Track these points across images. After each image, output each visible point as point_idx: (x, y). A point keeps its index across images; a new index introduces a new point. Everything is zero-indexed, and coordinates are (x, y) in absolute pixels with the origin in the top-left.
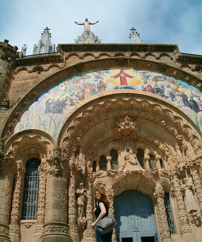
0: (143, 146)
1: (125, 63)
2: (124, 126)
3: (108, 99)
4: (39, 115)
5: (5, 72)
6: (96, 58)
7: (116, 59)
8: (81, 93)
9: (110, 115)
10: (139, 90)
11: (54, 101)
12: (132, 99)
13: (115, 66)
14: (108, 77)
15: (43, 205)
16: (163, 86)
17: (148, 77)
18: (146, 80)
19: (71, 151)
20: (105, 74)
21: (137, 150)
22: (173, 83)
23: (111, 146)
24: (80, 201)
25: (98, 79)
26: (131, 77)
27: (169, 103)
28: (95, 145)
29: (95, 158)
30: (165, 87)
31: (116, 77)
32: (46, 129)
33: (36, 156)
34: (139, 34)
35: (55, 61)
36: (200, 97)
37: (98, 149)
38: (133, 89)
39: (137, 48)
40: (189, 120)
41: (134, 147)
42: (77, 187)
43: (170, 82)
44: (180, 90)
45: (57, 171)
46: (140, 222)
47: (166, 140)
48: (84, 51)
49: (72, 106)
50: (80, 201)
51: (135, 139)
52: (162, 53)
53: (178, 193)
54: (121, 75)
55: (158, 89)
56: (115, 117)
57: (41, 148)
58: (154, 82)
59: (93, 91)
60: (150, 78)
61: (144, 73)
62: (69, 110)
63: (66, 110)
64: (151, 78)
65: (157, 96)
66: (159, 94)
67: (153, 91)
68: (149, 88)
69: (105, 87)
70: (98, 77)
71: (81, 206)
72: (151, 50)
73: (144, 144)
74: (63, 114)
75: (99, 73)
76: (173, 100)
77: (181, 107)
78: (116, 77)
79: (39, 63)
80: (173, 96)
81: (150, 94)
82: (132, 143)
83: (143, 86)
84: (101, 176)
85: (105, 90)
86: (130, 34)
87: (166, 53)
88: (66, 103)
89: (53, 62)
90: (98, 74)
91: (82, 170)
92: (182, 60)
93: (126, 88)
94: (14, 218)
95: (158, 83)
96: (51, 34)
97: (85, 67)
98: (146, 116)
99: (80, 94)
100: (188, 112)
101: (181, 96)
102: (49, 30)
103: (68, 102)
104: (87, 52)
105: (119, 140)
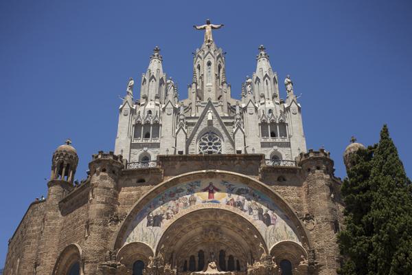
5: (113, 186)
9: (198, 225)
13: (206, 178)
17: (233, 189)
20: (197, 187)
23: (200, 248)
26: (218, 190)
48: (180, 161)
62: (166, 224)
65: (237, 211)
67: (234, 205)
69: (195, 201)
72: (240, 159)
78: (205, 190)
80: (251, 210)
81: (231, 208)
103: (165, 216)
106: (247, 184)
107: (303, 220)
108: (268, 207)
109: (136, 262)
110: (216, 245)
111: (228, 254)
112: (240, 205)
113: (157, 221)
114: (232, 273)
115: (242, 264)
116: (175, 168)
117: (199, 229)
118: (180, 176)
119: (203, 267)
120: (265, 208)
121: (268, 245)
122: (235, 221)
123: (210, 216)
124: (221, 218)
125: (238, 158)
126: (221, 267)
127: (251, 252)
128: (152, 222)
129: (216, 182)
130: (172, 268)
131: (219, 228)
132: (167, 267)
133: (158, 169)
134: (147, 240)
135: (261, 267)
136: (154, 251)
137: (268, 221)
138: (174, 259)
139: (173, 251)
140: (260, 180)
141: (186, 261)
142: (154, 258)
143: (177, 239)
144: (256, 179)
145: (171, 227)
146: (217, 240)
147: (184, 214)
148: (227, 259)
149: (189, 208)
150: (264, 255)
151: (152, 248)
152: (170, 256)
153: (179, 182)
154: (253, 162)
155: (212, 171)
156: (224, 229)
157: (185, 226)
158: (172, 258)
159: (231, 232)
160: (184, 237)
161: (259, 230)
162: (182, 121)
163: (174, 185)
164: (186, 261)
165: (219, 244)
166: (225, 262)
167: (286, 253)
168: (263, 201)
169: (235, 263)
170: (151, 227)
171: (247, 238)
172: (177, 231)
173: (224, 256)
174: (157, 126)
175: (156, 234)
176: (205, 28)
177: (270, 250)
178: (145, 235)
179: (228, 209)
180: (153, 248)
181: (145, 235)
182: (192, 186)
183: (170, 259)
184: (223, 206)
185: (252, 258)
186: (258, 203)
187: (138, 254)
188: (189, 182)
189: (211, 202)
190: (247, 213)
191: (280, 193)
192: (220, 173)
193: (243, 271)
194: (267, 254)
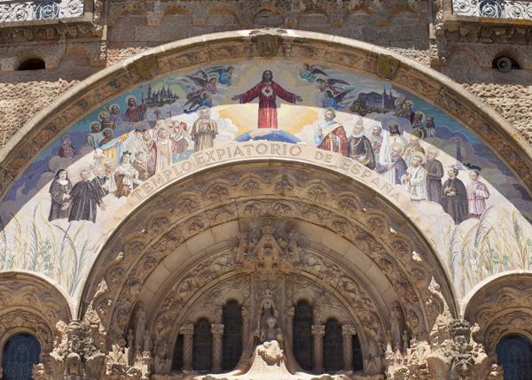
0: (313, 295)
1: (280, 50)
4: (34, 226)
8: (145, 155)
9: (223, 217)
11: (74, 181)
13: (250, 57)
14: (224, 97)
17: (340, 98)
19: (115, 323)
20: (219, 86)
21: (293, 309)
22: (412, 118)
23: (228, 293)
25: (198, 105)
26: (291, 98)
28: (183, 294)
29: (182, 328)
32: (50, 267)
33: (33, 333)
35: (77, 37)
38: (288, 141)
41: (286, 296)
47: (374, 285)
49: (119, 197)
51: (293, 274)
54: (263, 91)
55: (362, 142)
56: (238, 219)
57: (40, 315)
59: (180, 146)
61: (332, 81)
62: (113, 211)
63: (103, 209)
65: (355, 169)
66: (362, 158)
67: (346, 149)
68: (338, 139)
69: (213, 134)
70: (199, 97)
73: (316, 289)
74: (94, 222)
76: (398, 182)
77: (416, 203)
78: (246, 98)
79: (32, 40)
80: (401, 166)
81: (334, 161)
83: (321, 130)
85: (212, 146)
88: (103, 186)
89: (73, 40)
97: (161, 65)
99: (145, 158)
101: (423, 165)
103: (110, 185)
105: (249, 275)
106: (390, 78)
108: (459, 157)
109: (14, 337)
110: (282, 284)
111: (322, 314)
112: (363, 148)
113: (82, 201)
114: (335, 377)
115: (369, 349)
116: (146, 21)
117: (227, 230)
118: (163, 48)
119: (235, 358)
120: (448, 161)
121: (456, 285)
122: (346, 203)
123: (263, 186)
124: (301, 193)
126: (299, 357)
127: (400, 308)
128: (66, 206)
129: (286, 73)
130: (132, 361)
131: (291, 226)
132: (117, 356)
133: (88, 25)
134: (50, 267)
135: (431, 360)
136: (74, 302)
137: (457, 204)
138: (140, 328)
139: (137, 307)
140: (435, 65)
141: (181, 337)
142: (73, 326)
143: (151, 262)
144: (419, 61)
145: (129, 224)
146: (287, 266)
147: (175, 178)
148: (318, 331)
150: (444, 319)
151: (63, 289)
152: (125, 320)
153: (159, 71)
155: (273, 32)
156: (310, 229)
157: (178, 218)
158: (132, 326)
159: (333, 242)
160: (175, 258)
161: (429, 237)
163: (142, 78)
164: (181, 337)
165: (293, 279)
166: (312, 337)
167: (518, 314)
168: (443, 137)
170: (64, 222)
171: (387, 262)
172: (152, 238)
173: (311, 321)
175: (78, 244)
177: (463, 302)
178: (43, 250)
179: (319, 163)
180: (71, 291)
181: (43, 250)
182: (201, 82)
183: (128, 331)
184: (307, 153)
185: (403, 327)
186: (425, 144)
187: (18, 313)
188: (193, 70)
189: (268, 137)
191: (499, 110)
192: (297, 41)
193: (372, 374)
194: (454, 313)
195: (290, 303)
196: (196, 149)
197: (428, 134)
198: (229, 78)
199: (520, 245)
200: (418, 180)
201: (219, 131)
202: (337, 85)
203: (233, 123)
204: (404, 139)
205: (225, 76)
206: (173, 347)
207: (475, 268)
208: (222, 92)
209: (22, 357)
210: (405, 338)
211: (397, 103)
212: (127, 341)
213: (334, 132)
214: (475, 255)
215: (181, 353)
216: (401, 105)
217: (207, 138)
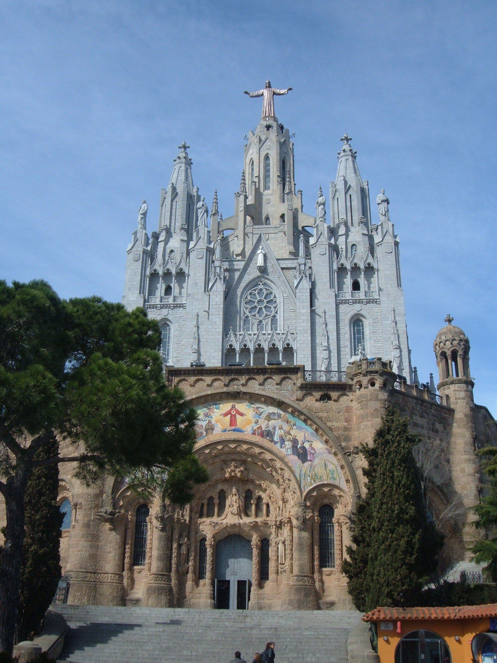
2: (230, 473)
3: (213, 446)
6: (208, 386)
7: (228, 393)
9: (217, 460)
10: (247, 435)
12: (239, 445)
13: (227, 399)
14: (217, 415)
15: (150, 555)
16: (274, 428)
17: (260, 414)
18: (258, 419)
20: (215, 410)
21: (245, 494)
22: (288, 422)
23: (220, 487)
24: (184, 550)
26: (242, 415)
27: (276, 452)
28: (203, 488)
30: (277, 429)
31: (226, 415)
34: (356, 153)
36: (312, 442)
37: (207, 490)
39: (255, 371)
40: (293, 472)
42: (180, 536)
43: (284, 421)
44: (293, 432)
45: (161, 528)
46: (239, 567)
50: (184, 550)
51: (244, 480)
52: (284, 376)
53: (273, 544)
54: (232, 412)
56: (223, 460)
58: (266, 421)
60: (262, 416)
61: (258, 408)
64: (264, 416)
65: (265, 442)
66: (268, 438)
67: (262, 435)
68: (259, 431)
69: (213, 429)
71: (184, 554)
72: (271, 373)
75: (209, 409)
76: (281, 447)
77: (288, 456)
78: (226, 415)
80: (282, 441)
81: (257, 439)
82: (241, 484)
83: (253, 427)
84: (204, 524)
86: (339, 154)
87: (289, 376)
90: (208, 411)
91: (185, 521)
92: (306, 387)
93: (234, 430)
94: (126, 566)
95: (272, 423)
96: (190, 160)
97: (194, 403)
98: (253, 460)
100: (294, 462)
101: (291, 441)
102: (189, 147)
104: (198, 377)
107: (349, 455)
125: (269, 371)
149: (206, 438)
154: (289, 376)
162: (218, 270)
164: (203, 504)
169: (264, 507)
174: (181, 275)
176: (263, 94)
190: (278, 445)
195: (243, 491)
196: (206, 435)
197: (293, 428)
198: (219, 407)
199: (326, 472)
200: (289, 447)
201: (215, 428)
202: (259, 409)
203: (221, 425)
204: (284, 430)
205: (217, 406)
206: (200, 508)
207: (309, 481)
208: (216, 412)
209: (143, 513)
210: (284, 506)
211: (282, 416)
212: (181, 508)
213: (258, 428)
214: (309, 476)
215: (203, 510)
216: (284, 417)
217: (210, 431)
